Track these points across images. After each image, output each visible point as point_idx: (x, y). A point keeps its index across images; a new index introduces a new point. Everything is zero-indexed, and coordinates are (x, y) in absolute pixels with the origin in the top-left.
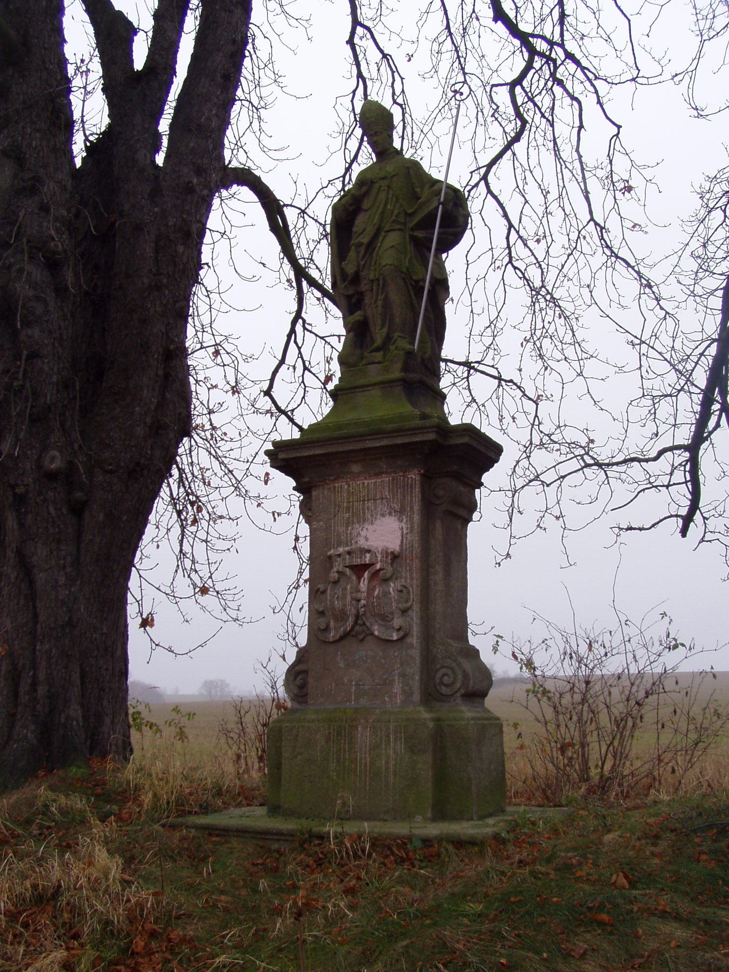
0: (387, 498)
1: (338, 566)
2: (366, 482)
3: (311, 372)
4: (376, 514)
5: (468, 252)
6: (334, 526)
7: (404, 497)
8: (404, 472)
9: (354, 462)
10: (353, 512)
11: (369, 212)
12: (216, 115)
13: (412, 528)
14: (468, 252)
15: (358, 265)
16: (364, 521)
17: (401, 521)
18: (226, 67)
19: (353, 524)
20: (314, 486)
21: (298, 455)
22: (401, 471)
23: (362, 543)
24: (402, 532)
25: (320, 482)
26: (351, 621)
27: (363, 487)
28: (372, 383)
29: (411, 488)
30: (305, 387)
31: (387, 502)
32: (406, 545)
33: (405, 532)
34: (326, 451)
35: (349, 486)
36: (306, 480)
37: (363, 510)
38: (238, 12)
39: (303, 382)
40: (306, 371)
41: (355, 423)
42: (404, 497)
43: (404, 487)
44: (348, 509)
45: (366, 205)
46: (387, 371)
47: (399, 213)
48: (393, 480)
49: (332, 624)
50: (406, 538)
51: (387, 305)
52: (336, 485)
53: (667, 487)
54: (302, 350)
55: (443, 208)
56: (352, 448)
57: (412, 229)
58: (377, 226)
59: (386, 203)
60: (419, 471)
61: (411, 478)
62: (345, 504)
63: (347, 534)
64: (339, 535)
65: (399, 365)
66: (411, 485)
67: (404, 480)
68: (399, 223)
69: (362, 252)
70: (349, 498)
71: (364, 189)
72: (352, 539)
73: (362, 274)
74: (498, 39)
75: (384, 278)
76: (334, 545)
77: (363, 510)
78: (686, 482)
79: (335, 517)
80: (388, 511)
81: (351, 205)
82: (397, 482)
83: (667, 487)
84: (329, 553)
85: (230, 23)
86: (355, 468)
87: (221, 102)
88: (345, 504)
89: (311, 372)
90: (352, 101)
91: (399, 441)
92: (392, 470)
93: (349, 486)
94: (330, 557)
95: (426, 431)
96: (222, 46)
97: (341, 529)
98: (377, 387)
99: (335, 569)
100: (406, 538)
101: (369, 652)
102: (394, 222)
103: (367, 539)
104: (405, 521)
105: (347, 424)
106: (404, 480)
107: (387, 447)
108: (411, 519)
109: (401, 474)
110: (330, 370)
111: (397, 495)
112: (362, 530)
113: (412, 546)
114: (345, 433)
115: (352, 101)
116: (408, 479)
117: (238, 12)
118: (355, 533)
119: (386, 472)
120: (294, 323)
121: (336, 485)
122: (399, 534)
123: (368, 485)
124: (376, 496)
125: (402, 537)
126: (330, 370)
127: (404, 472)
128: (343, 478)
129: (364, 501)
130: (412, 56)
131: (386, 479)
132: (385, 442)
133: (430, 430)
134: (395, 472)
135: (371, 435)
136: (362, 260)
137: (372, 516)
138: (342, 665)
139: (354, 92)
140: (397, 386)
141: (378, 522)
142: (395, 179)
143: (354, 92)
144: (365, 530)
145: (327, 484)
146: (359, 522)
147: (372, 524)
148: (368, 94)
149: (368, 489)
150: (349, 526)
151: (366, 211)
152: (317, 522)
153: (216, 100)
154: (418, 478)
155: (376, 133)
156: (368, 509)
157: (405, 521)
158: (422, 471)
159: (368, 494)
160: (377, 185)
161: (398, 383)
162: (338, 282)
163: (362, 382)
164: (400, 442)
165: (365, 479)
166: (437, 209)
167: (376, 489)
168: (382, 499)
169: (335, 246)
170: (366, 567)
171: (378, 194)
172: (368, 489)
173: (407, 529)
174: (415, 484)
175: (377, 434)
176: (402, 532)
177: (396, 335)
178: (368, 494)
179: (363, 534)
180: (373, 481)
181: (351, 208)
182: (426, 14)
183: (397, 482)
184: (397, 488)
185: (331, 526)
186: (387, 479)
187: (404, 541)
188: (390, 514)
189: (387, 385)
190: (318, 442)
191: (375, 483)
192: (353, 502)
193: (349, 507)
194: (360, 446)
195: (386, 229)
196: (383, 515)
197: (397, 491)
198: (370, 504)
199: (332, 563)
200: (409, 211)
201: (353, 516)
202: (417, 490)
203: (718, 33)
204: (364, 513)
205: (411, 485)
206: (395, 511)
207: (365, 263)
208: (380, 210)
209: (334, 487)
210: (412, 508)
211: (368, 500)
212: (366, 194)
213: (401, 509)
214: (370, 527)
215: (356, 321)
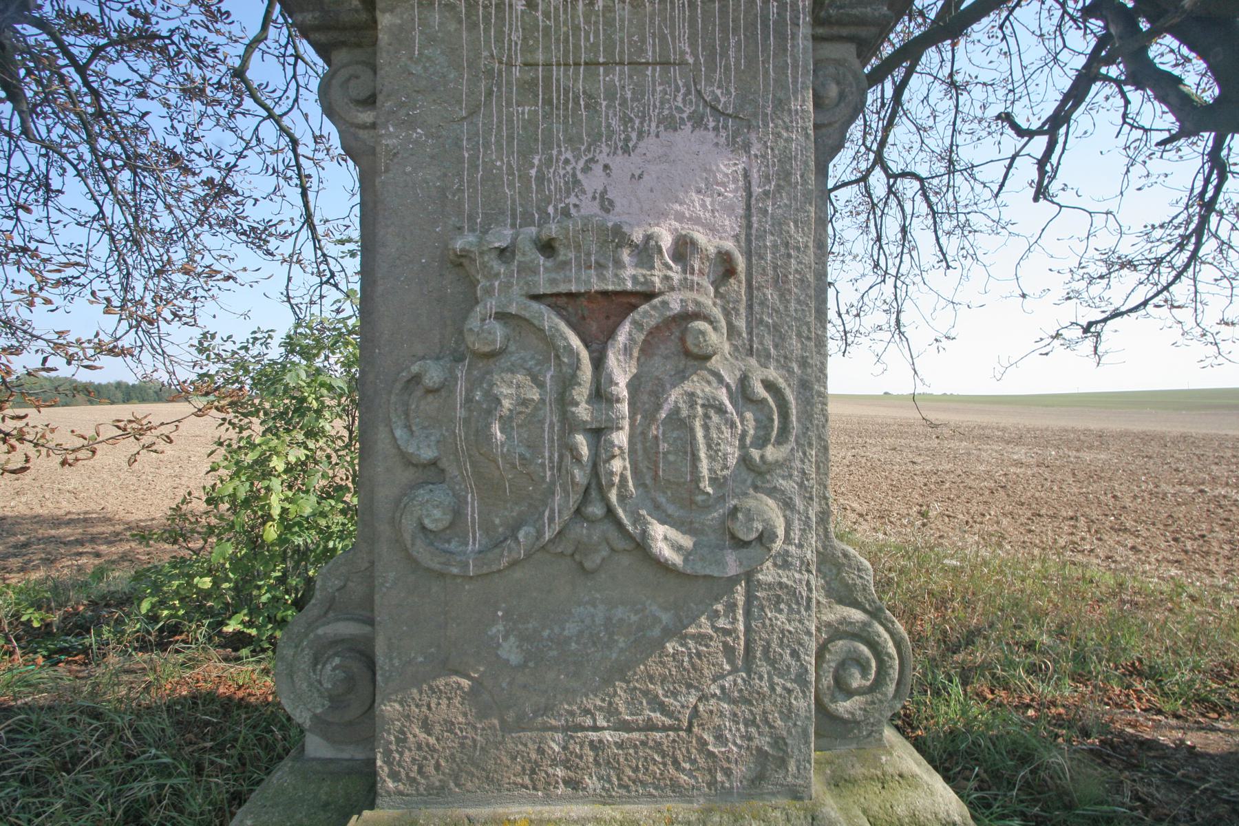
0: (683, 63)
7: (752, 60)
10: (548, 102)
16: (596, 139)
19: (548, 145)
26: (561, 504)
29: (781, 36)
33: (757, 190)
42: (752, 60)
44: (528, 87)
49: (472, 510)
63: (525, 179)
70: (527, 49)
76: (471, 218)
79: (473, 113)
84: (459, 244)
88: (516, 72)
94: (460, 262)
99: (492, 304)
101: (620, 612)
103: (607, 205)
111: (724, 54)
112: (587, 169)
118: (558, 175)
124: (642, 51)
137: (627, 120)
138: (511, 652)
141: (650, 145)
144: (598, 169)
147: (626, 150)
149: (609, 23)
150: (533, 152)
156: (611, 96)
168: (665, 64)
172: (609, 23)
179: (593, 182)
184: (724, 29)
188: (698, 122)
192: (548, 65)
193: (534, 82)
196: (671, 124)
199: (473, 284)
201: (547, 116)
204: (592, 107)
214: (618, 163)
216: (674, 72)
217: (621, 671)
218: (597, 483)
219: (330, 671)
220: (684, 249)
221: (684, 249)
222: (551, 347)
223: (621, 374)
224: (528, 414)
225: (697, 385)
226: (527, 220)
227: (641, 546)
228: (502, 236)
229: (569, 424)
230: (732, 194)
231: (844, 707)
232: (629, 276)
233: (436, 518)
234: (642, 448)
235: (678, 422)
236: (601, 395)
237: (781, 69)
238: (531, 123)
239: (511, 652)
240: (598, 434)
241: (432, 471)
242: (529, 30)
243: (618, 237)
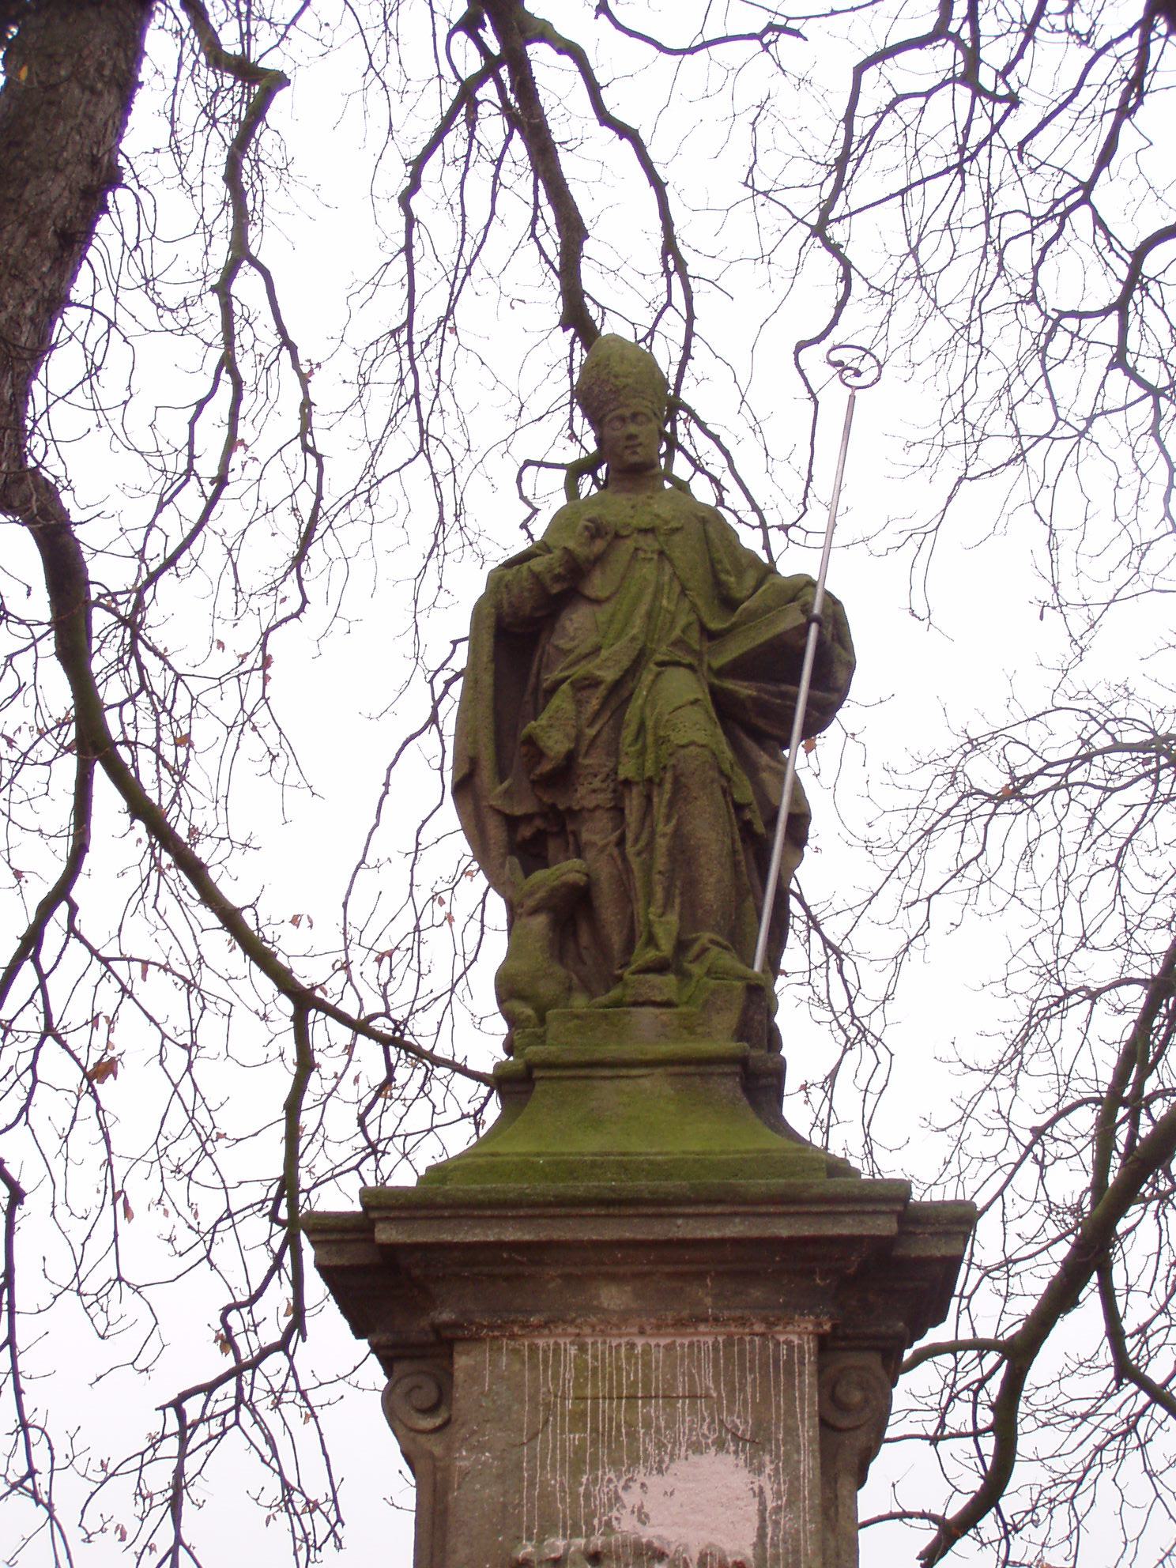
0: (708, 1396)
2: (640, 1342)
3: (64, 1045)
4: (675, 1442)
5: (424, 822)
6: (533, 1469)
7: (765, 1396)
8: (770, 1325)
9: (612, 1278)
10: (595, 1430)
11: (608, 608)
12: (32, 319)
13: (794, 1493)
14: (424, 822)
15: (578, 739)
16: (634, 1460)
17: (759, 1470)
18: (69, 214)
19: (594, 1465)
20: (463, 1339)
21: (446, 1237)
22: (764, 1320)
23: (627, 1524)
24: (762, 1503)
25: (491, 1327)
27: (628, 1359)
28: (649, 1057)
29: (790, 1373)
30: (35, 1081)
31: (709, 1408)
32: (775, 1545)
33: (770, 1505)
34: (543, 1236)
35: (582, 1348)
36: (446, 1316)
37: (630, 1425)
38: (111, 99)
39: (33, 1067)
40: (49, 1039)
41: (620, 1164)
42: (765, 1396)
43: (764, 1366)
44: (578, 1418)
45: (598, 584)
46: (691, 1030)
47: (689, 625)
48: (729, 1343)
50: (776, 1523)
51: (683, 852)
52: (541, 1342)
53: (934, 1440)
54: (48, 981)
55: (820, 633)
56: (628, 1235)
57: (720, 673)
58: (638, 645)
59: (657, 595)
60: (819, 1325)
61: (789, 1343)
62: (569, 1404)
63: (575, 1496)
64: (546, 1496)
65: (729, 1019)
66: (789, 1361)
67: (764, 1347)
68: (690, 650)
69: (594, 704)
70: (579, 1386)
71: (599, 545)
72: (593, 1514)
73: (587, 762)
74: (492, 382)
75: (676, 780)
76: (529, 1529)
77: (629, 1425)
78: (976, 1434)
80: (713, 1437)
81: (557, 578)
82: (742, 1353)
83: (934, 1440)
84: (521, 1554)
85: (92, 119)
86: (612, 1297)
87: (46, 294)
88: (569, 1404)
89: (64, 1045)
90: (192, 424)
91: (783, 1230)
92: (738, 1313)
93: (582, 1348)
95: (870, 1208)
96: (67, 163)
97: (557, 1480)
98: (659, 1071)
100: (776, 1523)
102: (677, 643)
103: (643, 1518)
104: (769, 1469)
105: (594, 1164)
106: (764, 1347)
107: (736, 1242)
108: (791, 1468)
109: (759, 1328)
110: (109, 1045)
111: (742, 1389)
112: (626, 1487)
113: (796, 1551)
114: (613, 1189)
115: (192, 424)
116: (777, 1344)
117: (111, 99)
118: (601, 1494)
119: (716, 1320)
120: (46, 910)
121: (541, 1342)
122: (754, 1507)
123: (647, 1351)
124: (674, 1387)
125: (763, 1520)
126: (109, 1045)
127: (770, 1325)
128: (572, 1322)
129: (631, 1398)
130: (319, 365)
131: (707, 1338)
132: (735, 1229)
133: (884, 1208)
134: (742, 1321)
135: (695, 1202)
136: (590, 725)
137: (660, 1446)
139: (201, 405)
140: (726, 1075)
141: (679, 1467)
142: (677, 538)
143: (201, 405)
144: (636, 1486)
145: (512, 1337)
146: (615, 1463)
147: (660, 1471)
148: (241, 415)
149: (647, 1365)
150: (582, 1472)
151: (598, 602)
152: (471, 1449)
153: (37, 285)
154: (810, 1345)
155: (635, 416)
156: (647, 1425)
157: (769, 1469)
158: (827, 1327)
159: (647, 1377)
160: (630, 544)
161: (727, 1069)
162: (486, 774)
163: (612, 1050)
164: (785, 1233)
165: (642, 1332)
166: (804, 631)
167: (674, 1367)
168: (693, 1397)
169: (487, 679)
171: (629, 566)
172: (647, 1365)
173: (778, 1495)
174: (802, 1363)
175: (719, 1201)
176: (762, 1503)
177: (706, 936)
178: (647, 1377)
180: (663, 1342)
181: (556, 589)
182: (370, 288)
183: (742, 1353)
184: (742, 1370)
185: (519, 1467)
186: (710, 1340)
187: (769, 1531)
188: (720, 1445)
189: (691, 1069)
190: (515, 1204)
191: (670, 1348)
192: (595, 1398)
193: (584, 1413)
194: (659, 1231)
195: (659, 657)
196: (697, 1448)
197: (743, 1377)
198: (654, 1409)
200: (714, 625)
201: (594, 1442)
202: (807, 1380)
203: (994, 470)
204: (632, 1435)
205: (789, 1361)
206: (736, 1438)
207: (599, 732)
208: (643, 609)
209: (533, 1349)
210: (791, 1432)
211: (647, 1397)
212: (599, 560)
213: (755, 1434)
214: (653, 1480)
215: (565, 885)
216: (701, 1404)
226: (576, 1532)
237: (790, 1401)
238: (579, 1450)
242: (580, 1369)
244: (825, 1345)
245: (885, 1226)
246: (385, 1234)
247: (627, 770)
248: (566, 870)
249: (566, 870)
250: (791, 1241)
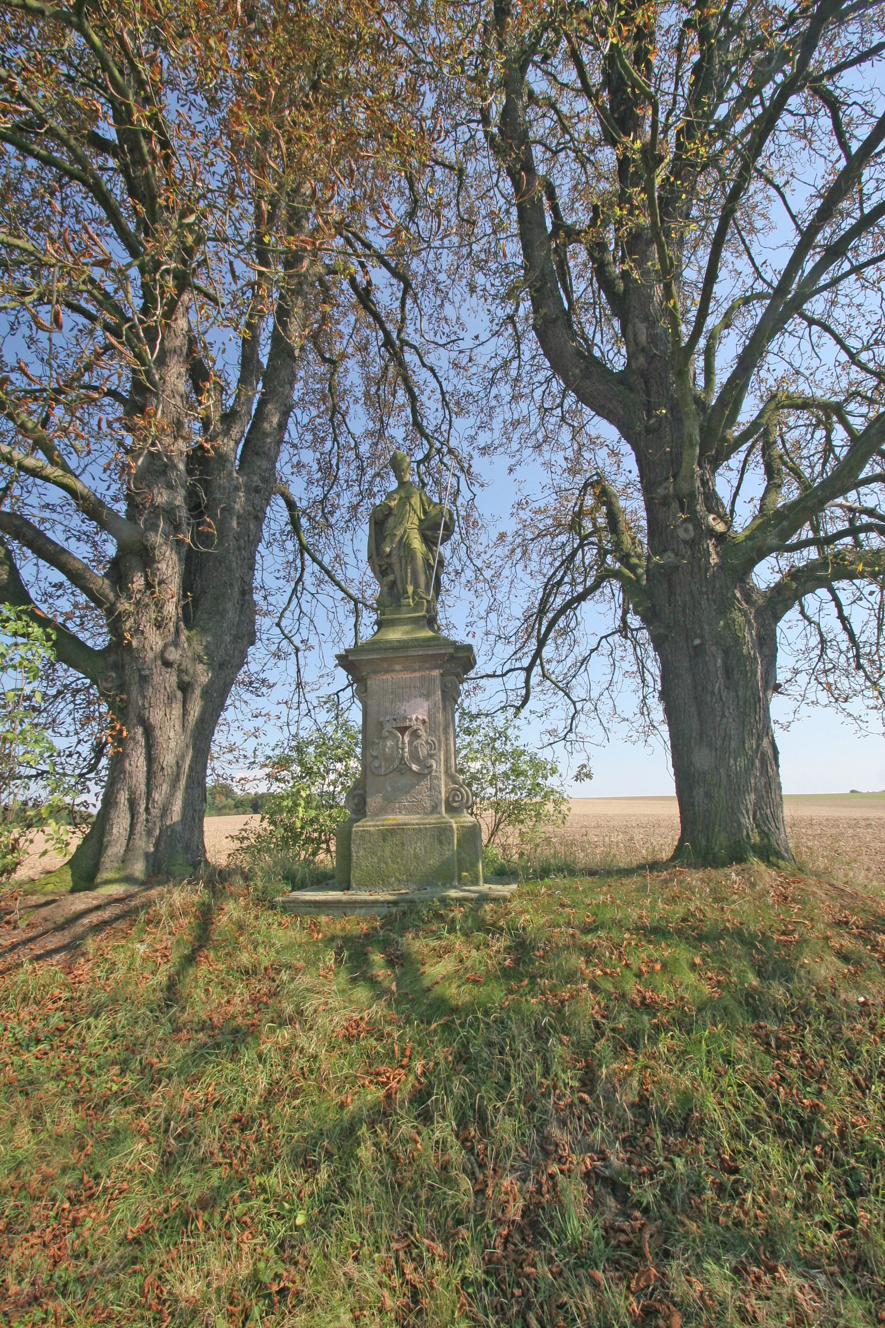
1: (388, 727)
26: (397, 762)
138: (389, 789)
141: (413, 701)
170: (406, 728)
217: (409, 792)
218: (402, 758)
219: (356, 801)
220: (417, 719)
221: (417, 719)
222: (395, 735)
223: (406, 739)
224: (392, 747)
225: (419, 741)
227: (411, 769)
228: (388, 718)
229: (398, 748)
230: (426, 708)
231: (455, 804)
232: (408, 724)
233: (377, 764)
234: (410, 752)
235: (416, 747)
236: (403, 743)
239: (389, 789)
240: (403, 749)
241: (376, 757)
243: (405, 718)
244: (442, 675)
245: (451, 650)
246: (351, 658)
247: (402, 554)
248: (391, 577)
249: (391, 577)
250: (432, 655)
